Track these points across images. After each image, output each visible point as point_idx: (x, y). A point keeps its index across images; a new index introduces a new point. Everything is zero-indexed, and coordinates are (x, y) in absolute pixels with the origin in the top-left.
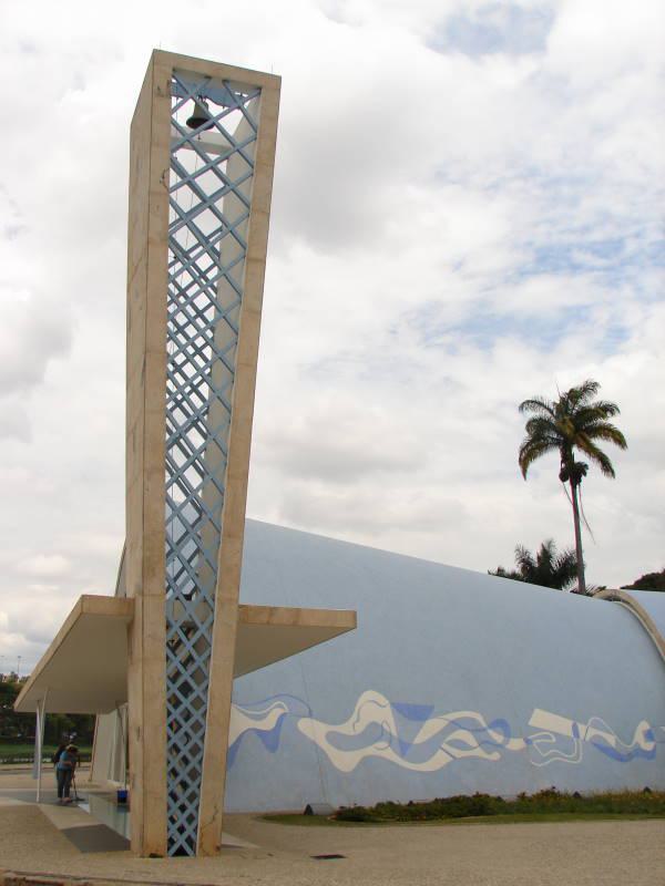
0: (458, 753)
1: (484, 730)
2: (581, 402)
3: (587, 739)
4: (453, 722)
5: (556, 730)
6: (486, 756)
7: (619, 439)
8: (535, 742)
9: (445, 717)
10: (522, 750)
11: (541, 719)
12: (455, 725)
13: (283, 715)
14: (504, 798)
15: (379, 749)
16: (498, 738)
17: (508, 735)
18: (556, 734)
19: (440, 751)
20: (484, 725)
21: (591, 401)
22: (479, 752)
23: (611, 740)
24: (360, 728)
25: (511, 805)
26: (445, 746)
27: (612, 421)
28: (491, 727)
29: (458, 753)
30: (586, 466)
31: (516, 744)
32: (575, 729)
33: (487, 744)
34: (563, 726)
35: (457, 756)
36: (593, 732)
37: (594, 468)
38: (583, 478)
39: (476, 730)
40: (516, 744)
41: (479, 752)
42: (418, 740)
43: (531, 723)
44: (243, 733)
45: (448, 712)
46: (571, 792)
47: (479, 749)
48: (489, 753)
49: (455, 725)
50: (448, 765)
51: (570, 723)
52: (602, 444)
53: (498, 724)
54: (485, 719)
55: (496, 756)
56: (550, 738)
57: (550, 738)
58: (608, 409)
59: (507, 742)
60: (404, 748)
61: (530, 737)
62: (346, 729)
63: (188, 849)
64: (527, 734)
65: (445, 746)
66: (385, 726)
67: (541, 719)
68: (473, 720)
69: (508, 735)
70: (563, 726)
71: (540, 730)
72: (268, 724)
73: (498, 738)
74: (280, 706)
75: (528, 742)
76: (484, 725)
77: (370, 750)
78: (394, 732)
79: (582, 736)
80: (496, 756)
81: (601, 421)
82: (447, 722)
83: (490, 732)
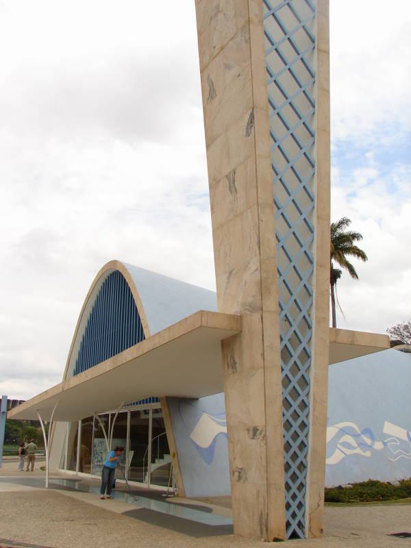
1: (359, 435)
2: (339, 231)
4: (341, 429)
5: (397, 436)
6: (363, 454)
7: (361, 255)
8: (389, 444)
9: (337, 425)
11: (390, 429)
12: (343, 431)
14: (343, 486)
16: (369, 441)
17: (373, 439)
18: (399, 439)
20: (359, 432)
21: (346, 230)
22: (358, 451)
25: (395, 489)
26: (339, 446)
27: (355, 243)
28: (363, 434)
29: (349, 452)
30: (340, 271)
31: (378, 446)
33: (362, 445)
35: (348, 453)
37: (345, 272)
38: (338, 280)
39: (355, 436)
40: (378, 446)
41: (358, 451)
44: (216, 436)
45: (337, 423)
46: (386, 481)
47: (359, 449)
48: (365, 452)
50: (343, 459)
51: (406, 431)
52: (350, 258)
53: (367, 431)
54: (359, 428)
55: (368, 454)
56: (396, 442)
58: (355, 236)
61: (386, 441)
63: (299, 532)
64: (383, 438)
65: (339, 446)
67: (390, 429)
68: (353, 428)
71: (390, 436)
73: (369, 441)
75: (385, 444)
76: (359, 432)
80: (368, 454)
81: (347, 244)
82: (338, 429)
83: (363, 436)
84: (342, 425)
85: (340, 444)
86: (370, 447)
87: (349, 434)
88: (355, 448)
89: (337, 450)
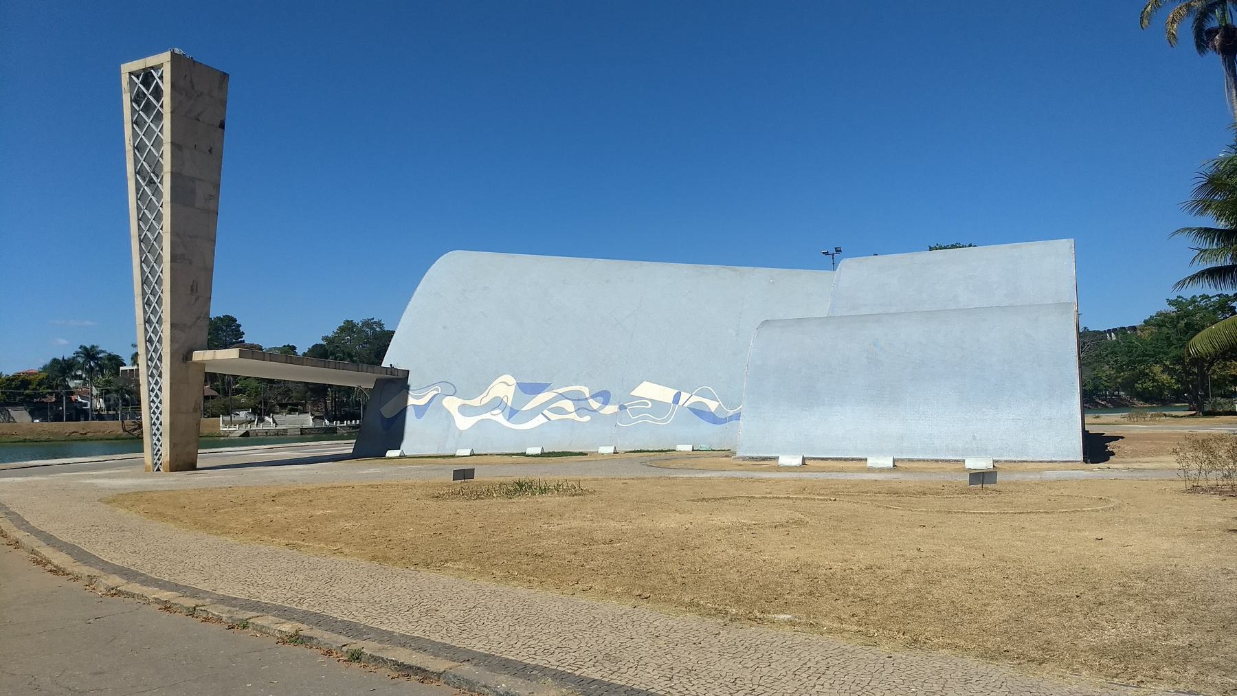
0: (554, 417)
1: (586, 399)
3: (686, 405)
6: (578, 419)
10: (616, 413)
11: (649, 391)
12: (563, 396)
13: (435, 395)
16: (595, 404)
19: (541, 415)
20: (588, 396)
22: (574, 416)
23: (713, 406)
24: (485, 401)
26: (545, 412)
28: (592, 397)
32: (676, 399)
34: (665, 394)
36: (695, 399)
39: (578, 399)
40: (611, 409)
41: (574, 416)
42: (525, 408)
43: (632, 393)
45: (558, 388)
49: (563, 396)
55: (587, 418)
59: (601, 408)
60: (512, 413)
62: (476, 402)
66: (505, 400)
69: (606, 403)
70: (665, 394)
74: (437, 390)
75: (622, 407)
76: (588, 396)
77: (487, 416)
78: (509, 404)
79: (681, 403)
83: (591, 401)
84: (561, 391)
85: (548, 410)
86: (595, 411)
87: (568, 399)
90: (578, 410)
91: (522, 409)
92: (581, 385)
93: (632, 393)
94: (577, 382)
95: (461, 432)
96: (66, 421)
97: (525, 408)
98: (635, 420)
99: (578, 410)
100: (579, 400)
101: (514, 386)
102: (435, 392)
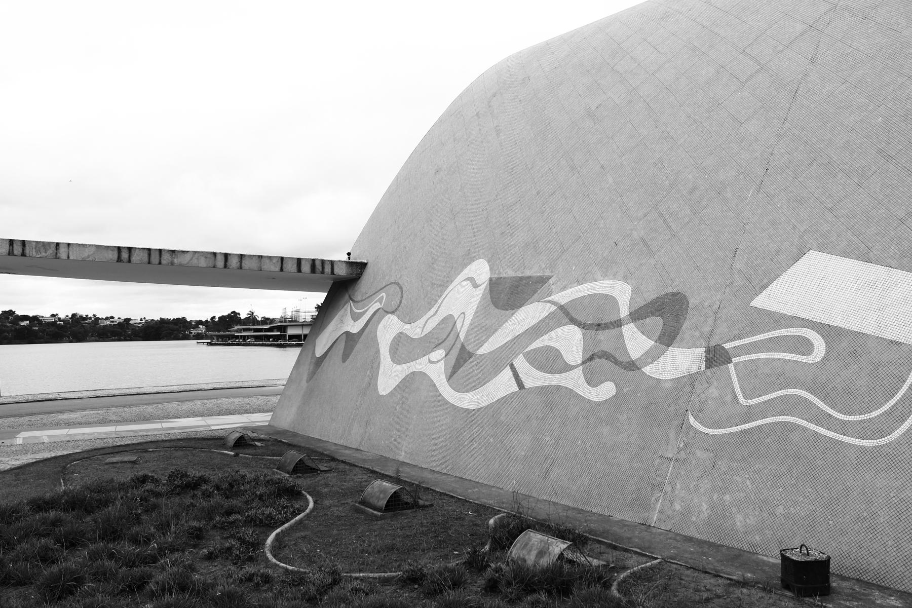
0: (534, 378)
4: (562, 308)
10: (692, 379)
15: (430, 362)
18: (829, 332)
20: (624, 312)
26: (520, 363)
28: (637, 316)
29: (534, 378)
35: (528, 383)
42: (484, 350)
55: (606, 391)
57: (805, 346)
59: (652, 356)
65: (520, 363)
66: (459, 325)
69: (668, 338)
72: (354, 327)
74: (380, 301)
77: (420, 365)
78: (462, 336)
80: (606, 391)
82: (554, 308)
83: (629, 331)
84: (564, 297)
86: (632, 366)
87: (573, 321)
88: (568, 368)
89: (508, 370)
90: (591, 358)
91: (478, 352)
92: (615, 277)
93: (759, 302)
94: (607, 268)
95: (379, 396)
96: (301, 335)
97: (484, 350)
98: (749, 414)
99: (591, 358)
100: (599, 327)
101: (483, 287)
102: (377, 306)
